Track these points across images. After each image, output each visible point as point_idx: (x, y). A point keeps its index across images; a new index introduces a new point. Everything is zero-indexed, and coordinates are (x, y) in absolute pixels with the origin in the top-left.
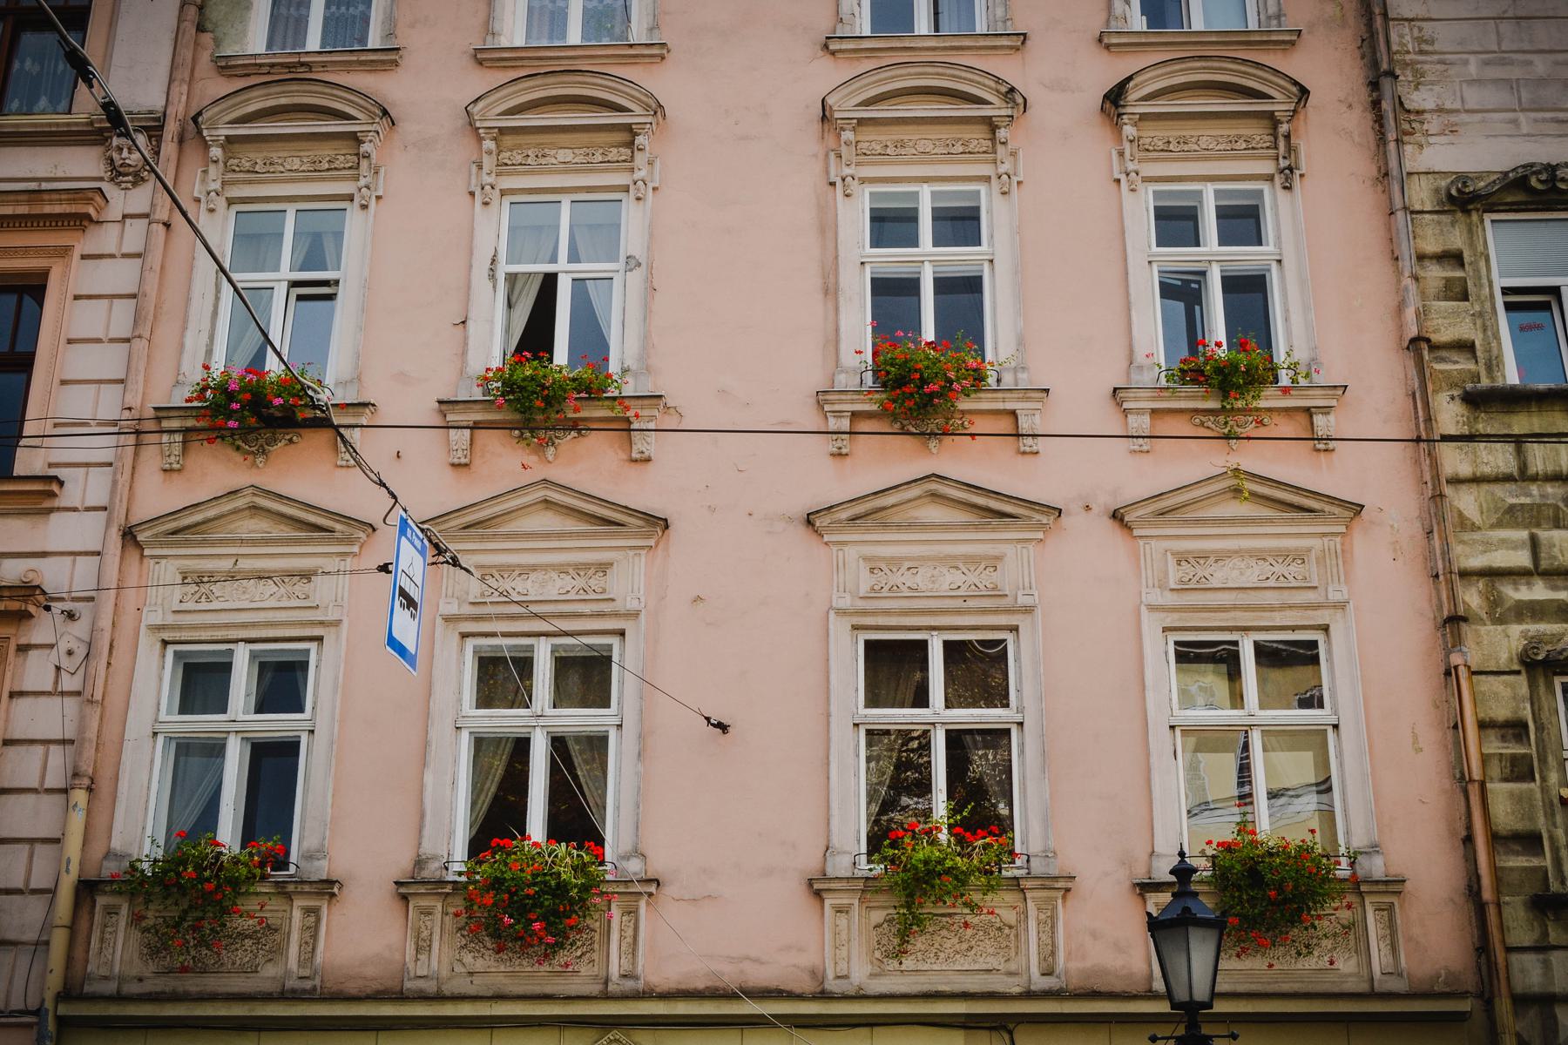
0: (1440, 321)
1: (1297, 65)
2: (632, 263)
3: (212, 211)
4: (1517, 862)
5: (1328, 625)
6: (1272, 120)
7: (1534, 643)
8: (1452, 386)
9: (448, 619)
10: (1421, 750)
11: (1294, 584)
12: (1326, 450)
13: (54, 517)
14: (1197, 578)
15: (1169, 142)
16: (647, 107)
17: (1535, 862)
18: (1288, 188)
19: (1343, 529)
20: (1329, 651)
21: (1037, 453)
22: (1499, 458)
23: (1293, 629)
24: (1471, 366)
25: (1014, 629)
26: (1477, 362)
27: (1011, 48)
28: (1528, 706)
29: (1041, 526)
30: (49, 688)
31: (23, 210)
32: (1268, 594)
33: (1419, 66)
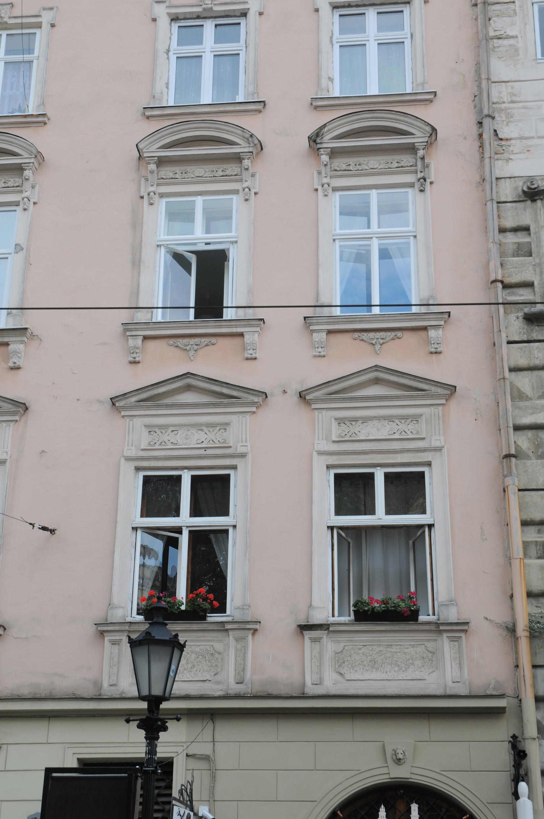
0: (512, 270)
5: (430, 462)
6: (412, 149)
10: (486, 539)
11: (411, 436)
12: (436, 353)
14: (350, 434)
16: (31, 153)
19: (443, 401)
20: (431, 478)
21: (255, 359)
26: (535, 294)
27: (256, 111)
29: (253, 404)
33: (510, 111)
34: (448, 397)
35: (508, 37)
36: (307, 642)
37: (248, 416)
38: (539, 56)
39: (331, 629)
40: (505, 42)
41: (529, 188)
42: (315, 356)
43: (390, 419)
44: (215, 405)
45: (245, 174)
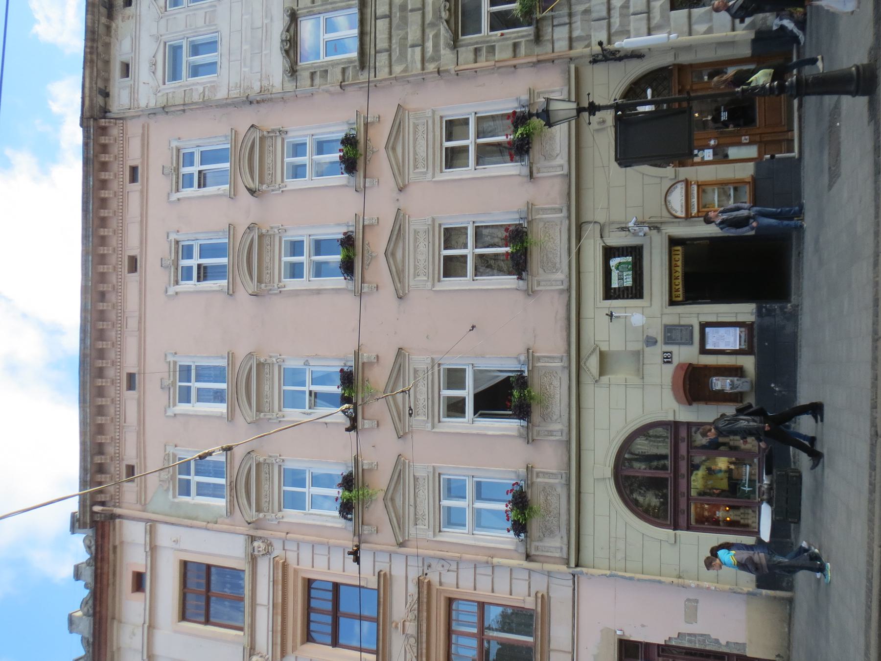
1: (243, 129)
2: (306, 363)
3: (283, 517)
4: (522, 50)
6: (262, 139)
7: (447, 45)
8: (357, 75)
9: (433, 427)
13: (393, 573)
15: (269, 174)
17: (523, 44)
18: (287, 132)
20: (449, 116)
22: (383, 59)
23: (441, 128)
24: (351, 68)
25: (440, 225)
27: (234, 229)
28: (469, 47)
29: (404, 216)
30: (456, 573)
31: (280, 587)
32: (429, 136)
34: (404, 110)
35: (204, 92)
36: (540, 175)
37: (411, 219)
38: (216, 75)
39: (531, 161)
40: (206, 93)
41: (289, 73)
42: (378, 184)
43: (415, 140)
44: (404, 238)
45: (271, 232)
